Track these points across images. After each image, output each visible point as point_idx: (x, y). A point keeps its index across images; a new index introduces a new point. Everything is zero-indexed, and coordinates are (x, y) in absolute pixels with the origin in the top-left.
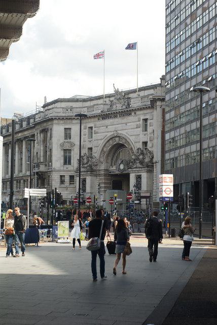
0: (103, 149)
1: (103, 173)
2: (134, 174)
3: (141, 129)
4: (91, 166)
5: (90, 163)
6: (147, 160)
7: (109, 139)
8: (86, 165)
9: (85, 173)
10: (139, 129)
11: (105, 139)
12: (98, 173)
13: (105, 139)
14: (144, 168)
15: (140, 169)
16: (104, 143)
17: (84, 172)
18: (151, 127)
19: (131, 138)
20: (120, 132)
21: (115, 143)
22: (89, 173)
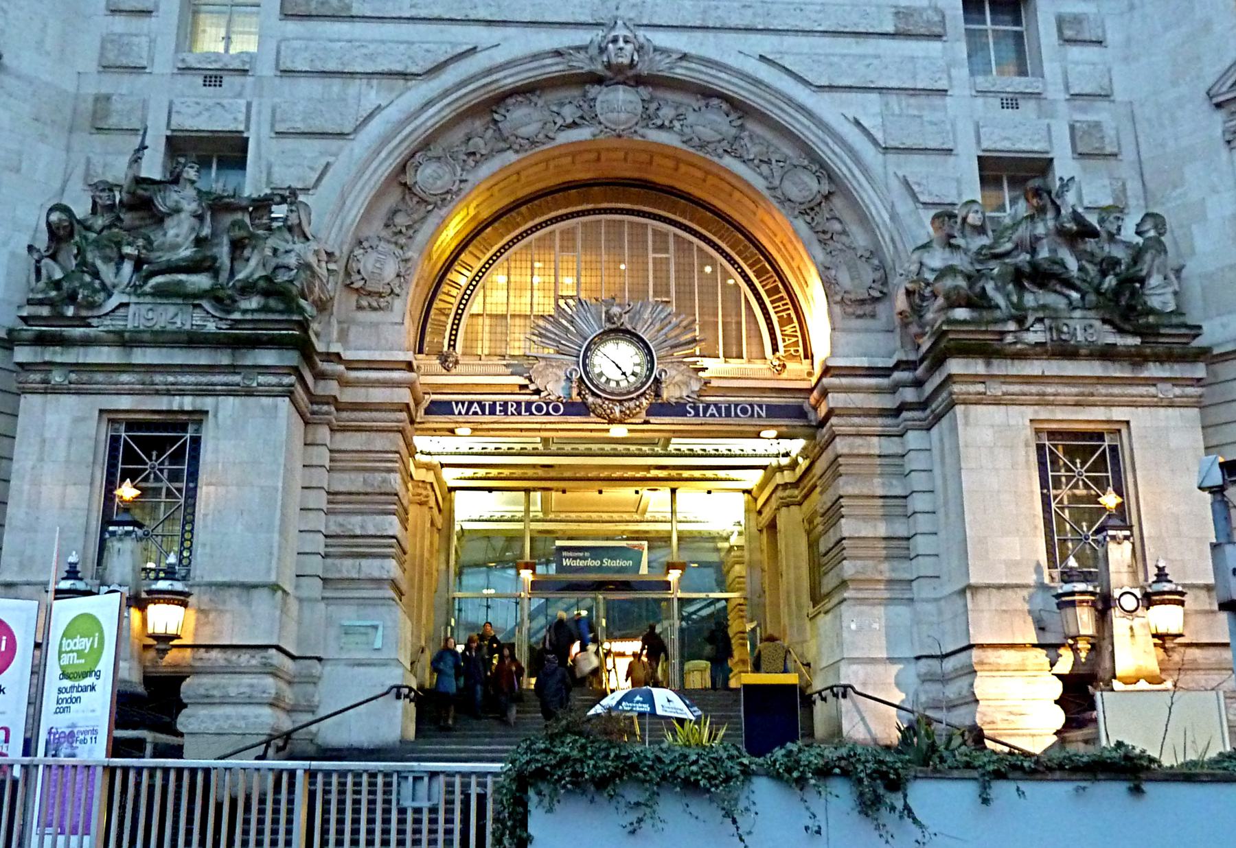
0: (403, 168)
1: (404, 396)
2: (1021, 419)
3: (962, 49)
4: (270, 289)
5: (251, 268)
6: (1159, 296)
7: (509, 80)
8: (202, 281)
9: (224, 358)
10: (936, 46)
11: (450, 76)
12: (332, 388)
13: (450, 76)
14: (1160, 359)
15: (1116, 370)
16: (431, 118)
17: (194, 340)
18: (1075, 52)
19: (826, 107)
20: (661, 39)
21: (583, 134)
22: (268, 357)
